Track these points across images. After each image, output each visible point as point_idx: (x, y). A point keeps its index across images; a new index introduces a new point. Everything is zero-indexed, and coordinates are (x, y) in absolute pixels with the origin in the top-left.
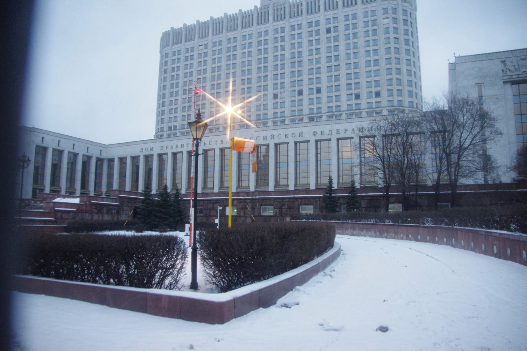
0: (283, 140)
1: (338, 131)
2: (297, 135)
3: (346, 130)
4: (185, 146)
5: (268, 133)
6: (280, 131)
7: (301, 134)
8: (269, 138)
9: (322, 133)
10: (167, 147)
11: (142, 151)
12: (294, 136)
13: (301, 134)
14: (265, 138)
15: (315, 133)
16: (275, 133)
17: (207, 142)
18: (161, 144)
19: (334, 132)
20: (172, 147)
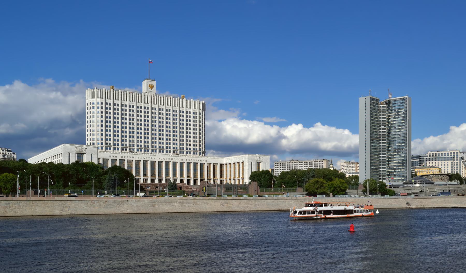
0: (176, 161)
1: (194, 160)
3: (196, 160)
4: (134, 157)
5: (171, 158)
6: (175, 157)
7: (182, 160)
8: (171, 159)
9: (189, 160)
10: (125, 157)
11: (110, 157)
14: (169, 159)
15: (187, 160)
16: (173, 157)
17: (145, 158)
18: (122, 155)
19: (193, 160)
20: (127, 157)
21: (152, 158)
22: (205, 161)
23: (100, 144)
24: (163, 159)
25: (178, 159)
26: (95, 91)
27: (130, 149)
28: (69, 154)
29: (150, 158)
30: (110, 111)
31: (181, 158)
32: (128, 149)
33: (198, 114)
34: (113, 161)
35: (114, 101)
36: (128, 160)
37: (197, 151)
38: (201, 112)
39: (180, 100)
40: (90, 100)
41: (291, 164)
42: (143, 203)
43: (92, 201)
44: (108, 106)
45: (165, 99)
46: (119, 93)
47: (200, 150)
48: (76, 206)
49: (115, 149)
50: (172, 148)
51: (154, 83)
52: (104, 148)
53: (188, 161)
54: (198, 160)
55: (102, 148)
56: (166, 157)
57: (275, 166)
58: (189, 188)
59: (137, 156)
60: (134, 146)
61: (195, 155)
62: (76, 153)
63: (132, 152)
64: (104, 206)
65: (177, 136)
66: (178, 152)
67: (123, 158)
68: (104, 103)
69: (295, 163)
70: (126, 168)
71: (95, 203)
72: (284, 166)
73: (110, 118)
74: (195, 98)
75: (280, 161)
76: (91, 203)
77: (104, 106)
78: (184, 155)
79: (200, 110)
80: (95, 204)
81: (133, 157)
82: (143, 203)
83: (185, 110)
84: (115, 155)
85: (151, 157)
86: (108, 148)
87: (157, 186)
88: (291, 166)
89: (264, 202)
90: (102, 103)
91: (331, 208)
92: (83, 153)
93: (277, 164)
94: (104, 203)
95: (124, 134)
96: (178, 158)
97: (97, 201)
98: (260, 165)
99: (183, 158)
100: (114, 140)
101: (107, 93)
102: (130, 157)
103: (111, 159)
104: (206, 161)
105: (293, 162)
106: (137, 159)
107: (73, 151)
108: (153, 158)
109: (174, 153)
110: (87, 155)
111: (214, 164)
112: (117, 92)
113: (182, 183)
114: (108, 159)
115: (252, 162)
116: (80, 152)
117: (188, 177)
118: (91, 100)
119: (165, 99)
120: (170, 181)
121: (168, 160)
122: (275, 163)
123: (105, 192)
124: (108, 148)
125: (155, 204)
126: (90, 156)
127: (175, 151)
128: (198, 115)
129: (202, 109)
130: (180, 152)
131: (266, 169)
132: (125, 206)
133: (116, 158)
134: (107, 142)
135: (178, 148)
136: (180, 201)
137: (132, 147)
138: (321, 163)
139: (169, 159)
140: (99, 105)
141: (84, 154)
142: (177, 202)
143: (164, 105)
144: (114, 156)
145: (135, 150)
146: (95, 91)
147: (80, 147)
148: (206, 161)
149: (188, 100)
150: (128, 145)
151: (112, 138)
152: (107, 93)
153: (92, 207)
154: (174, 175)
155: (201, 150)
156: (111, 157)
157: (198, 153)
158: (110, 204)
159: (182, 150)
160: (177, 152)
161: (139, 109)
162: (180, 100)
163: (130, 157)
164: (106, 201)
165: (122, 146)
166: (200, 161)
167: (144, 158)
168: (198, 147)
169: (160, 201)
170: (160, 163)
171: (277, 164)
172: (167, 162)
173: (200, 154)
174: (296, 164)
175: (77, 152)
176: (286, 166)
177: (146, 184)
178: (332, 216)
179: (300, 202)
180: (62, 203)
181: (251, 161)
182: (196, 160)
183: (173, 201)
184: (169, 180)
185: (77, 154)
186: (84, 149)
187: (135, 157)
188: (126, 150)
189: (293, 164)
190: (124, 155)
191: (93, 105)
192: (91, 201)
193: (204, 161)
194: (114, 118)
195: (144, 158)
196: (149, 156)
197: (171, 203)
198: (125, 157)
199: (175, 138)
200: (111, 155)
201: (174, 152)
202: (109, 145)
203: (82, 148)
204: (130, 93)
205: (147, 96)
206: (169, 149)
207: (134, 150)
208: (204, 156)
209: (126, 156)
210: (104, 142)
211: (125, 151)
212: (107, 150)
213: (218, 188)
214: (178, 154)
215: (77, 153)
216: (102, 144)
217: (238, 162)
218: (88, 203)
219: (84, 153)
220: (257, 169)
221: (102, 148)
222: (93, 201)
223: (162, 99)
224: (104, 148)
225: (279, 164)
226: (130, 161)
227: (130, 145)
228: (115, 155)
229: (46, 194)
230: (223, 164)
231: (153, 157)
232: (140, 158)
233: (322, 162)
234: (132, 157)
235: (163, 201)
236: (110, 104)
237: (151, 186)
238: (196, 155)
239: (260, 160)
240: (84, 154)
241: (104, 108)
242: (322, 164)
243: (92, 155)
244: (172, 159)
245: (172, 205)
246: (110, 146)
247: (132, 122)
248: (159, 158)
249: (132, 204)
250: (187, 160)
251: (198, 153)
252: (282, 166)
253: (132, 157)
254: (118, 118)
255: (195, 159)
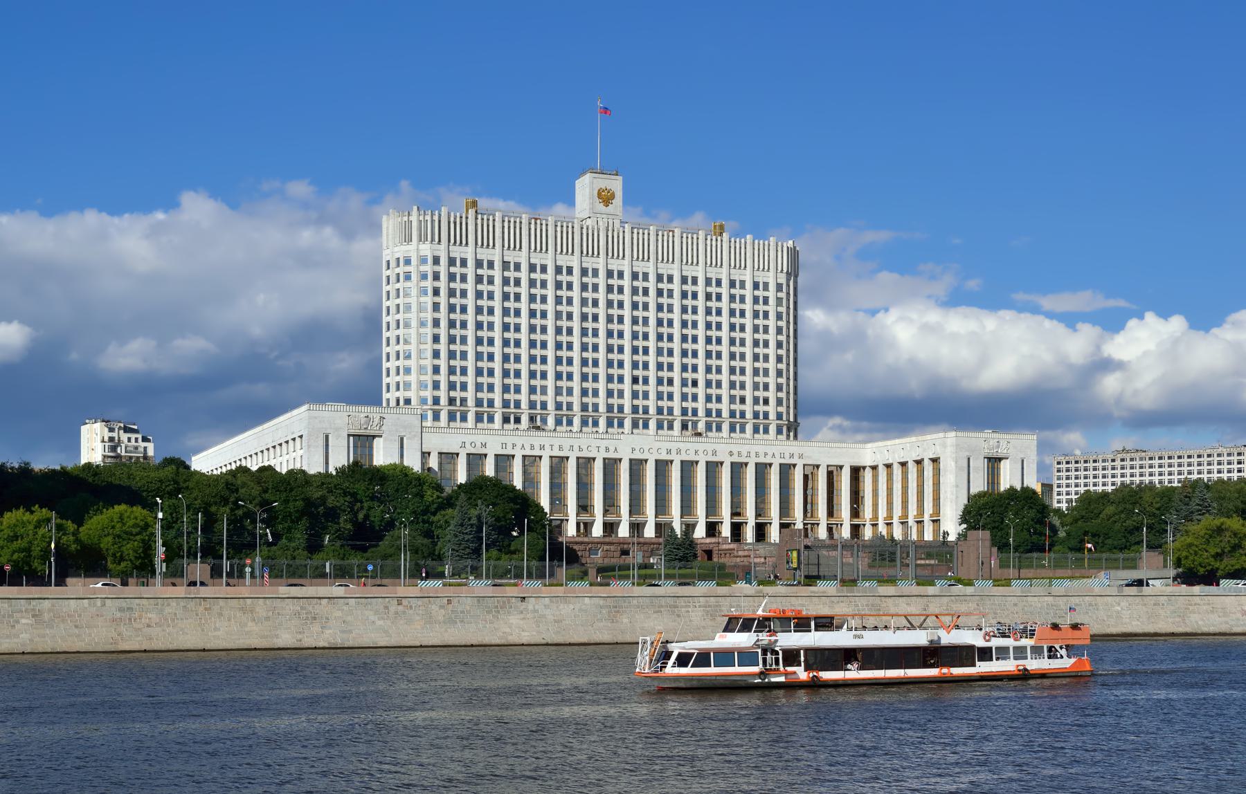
0: (691, 457)
1: (757, 455)
2: (710, 453)
3: (766, 454)
5: (674, 446)
6: (689, 445)
7: (714, 453)
8: (674, 452)
9: (739, 453)
10: (514, 446)
11: (463, 445)
12: (705, 453)
13: (714, 453)
14: (669, 452)
16: (681, 445)
18: (503, 439)
19: (753, 455)
21: (607, 449)
22: (796, 456)
23: (430, 401)
24: (646, 451)
25: (701, 450)
26: (414, 218)
27: (532, 419)
28: (327, 437)
29: (602, 450)
30: (464, 286)
31: (710, 447)
32: (525, 419)
33: (772, 287)
34: (475, 460)
35: (479, 250)
36: (524, 457)
37: (767, 421)
38: (782, 279)
39: (709, 242)
40: (396, 249)
41: (1118, 463)
42: (578, 606)
43: (403, 600)
44: (457, 270)
45: (653, 238)
46: (496, 224)
47: (779, 416)
48: (349, 618)
49: (479, 418)
50: (677, 411)
51: (616, 184)
52: (444, 416)
53: (736, 459)
54: (770, 454)
55: (436, 417)
56: (658, 444)
57: (1059, 471)
58: (740, 553)
59: (557, 442)
60: (544, 405)
61: (761, 436)
62: (349, 435)
63: (538, 428)
64: (441, 618)
65: (695, 369)
66: (701, 427)
67: (509, 451)
68: (444, 261)
69: (1132, 460)
70: (518, 483)
71: (411, 607)
72: (1091, 473)
73: (464, 309)
74: (760, 234)
75: (1078, 452)
76: (400, 608)
77: (443, 269)
78: (721, 435)
79: (779, 275)
80: (411, 612)
81: (542, 447)
82: (578, 606)
83: (576, 262)
84: (479, 439)
85: (603, 444)
86: (458, 414)
87: (626, 546)
88: (1118, 472)
89: (1015, 605)
90: (436, 261)
91: (855, 636)
92: (372, 433)
93: (1064, 466)
94: (442, 607)
95: (511, 366)
96: (700, 447)
97: (420, 602)
98: (998, 469)
99: (718, 447)
100: (479, 387)
101: (455, 223)
102: (532, 447)
103: (467, 454)
104: (801, 456)
105: (1128, 456)
106: (556, 453)
107: (337, 429)
108: (612, 449)
109: (687, 429)
110: (385, 440)
111: (828, 466)
112: (488, 220)
113: (714, 536)
114: (458, 454)
115: (969, 459)
116: (362, 432)
117: (735, 514)
118: (401, 251)
119: (653, 238)
120: (672, 529)
121: (664, 457)
122: (1059, 463)
123: (447, 570)
124: (458, 414)
125: (618, 612)
126: (397, 445)
127: (690, 423)
128: (771, 294)
129: (785, 270)
130: (709, 427)
131: (1023, 483)
132: (514, 619)
133: (483, 451)
134: (453, 394)
135: (701, 413)
136: (707, 602)
137: (539, 412)
138: (1235, 458)
139: (669, 452)
140: (428, 268)
141: (374, 437)
142: (697, 605)
143: (651, 260)
144: (479, 445)
145: (551, 421)
146: (414, 218)
147: (363, 415)
148: (801, 456)
149: (738, 240)
150: (524, 405)
151: (470, 379)
152: (455, 223)
153: (402, 622)
154: (687, 506)
155: (781, 419)
156: (468, 445)
157: (773, 429)
158: (462, 612)
159: (714, 418)
160: (695, 424)
161: (564, 278)
162: (709, 242)
163: (532, 447)
164: (449, 602)
165: (504, 407)
166: (777, 455)
167: (580, 449)
168: (771, 409)
169: (635, 602)
170: (637, 466)
171: (1064, 466)
172: (609, 459)
173: (779, 431)
174: (1137, 463)
175: (352, 432)
176: (1100, 473)
177: (586, 539)
178: (853, 673)
179: (1155, 605)
180: (302, 608)
181: (967, 454)
182: (766, 454)
183: (681, 602)
184: (669, 525)
185: (351, 438)
186: (377, 420)
187: (548, 444)
188: (518, 420)
189: (1128, 463)
190: (509, 440)
191: (408, 269)
192: (400, 600)
193: (792, 456)
194: (479, 310)
195: (580, 449)
196: (599, 443)
197: (676, 607)
198: (514, 446)
199: (689, 375)
200: (468, 439)
201: (684, 426)
202: (461, 405)
203: (367, 417)
204: (533, 221)
205: (593, 231)
206: (668, 414)
207: (544, 421)
208: (792, 438)
209: (519, 441)
210: (443, 394)
211: (516, 426)
212: (452, 424)
213: (844, 553)
214: (700, 434)
215: (353, 435)
216: (436, 401)
217: (919, 458)
218: (386, 608)
219: (376, 433)
220: (988, 483)
221: (436, 417)
222: (405, 602)
223: (643, 239)
224: (444, 416)
225: (1072, 466)
226: (530, 462)
227: (532, 405)
228: (479, 439)
229: (248, 575)
230: (864, 468)
231: (611, 444)
232: (566, 447)
233: (1239, 454)
234: (537, 447)
235: (647, 600)
236: (464, 263)
237: (606, 547)
238: (766, 436)
239: (1001, 452)
240: (374, 437)
241: (444, 277)
242: (1239, 463)
243: (402, 440)
244: (679, 452)
245: (679, 616)
246: (462, 408)
247: (538, 322)
248: (633, 450)
249: (535, 611)
250: (731, 454)
251: (773, 429)
252: (1082, 473)
253: (537, 447)
254: (491, 311)
255: (761, 449)
